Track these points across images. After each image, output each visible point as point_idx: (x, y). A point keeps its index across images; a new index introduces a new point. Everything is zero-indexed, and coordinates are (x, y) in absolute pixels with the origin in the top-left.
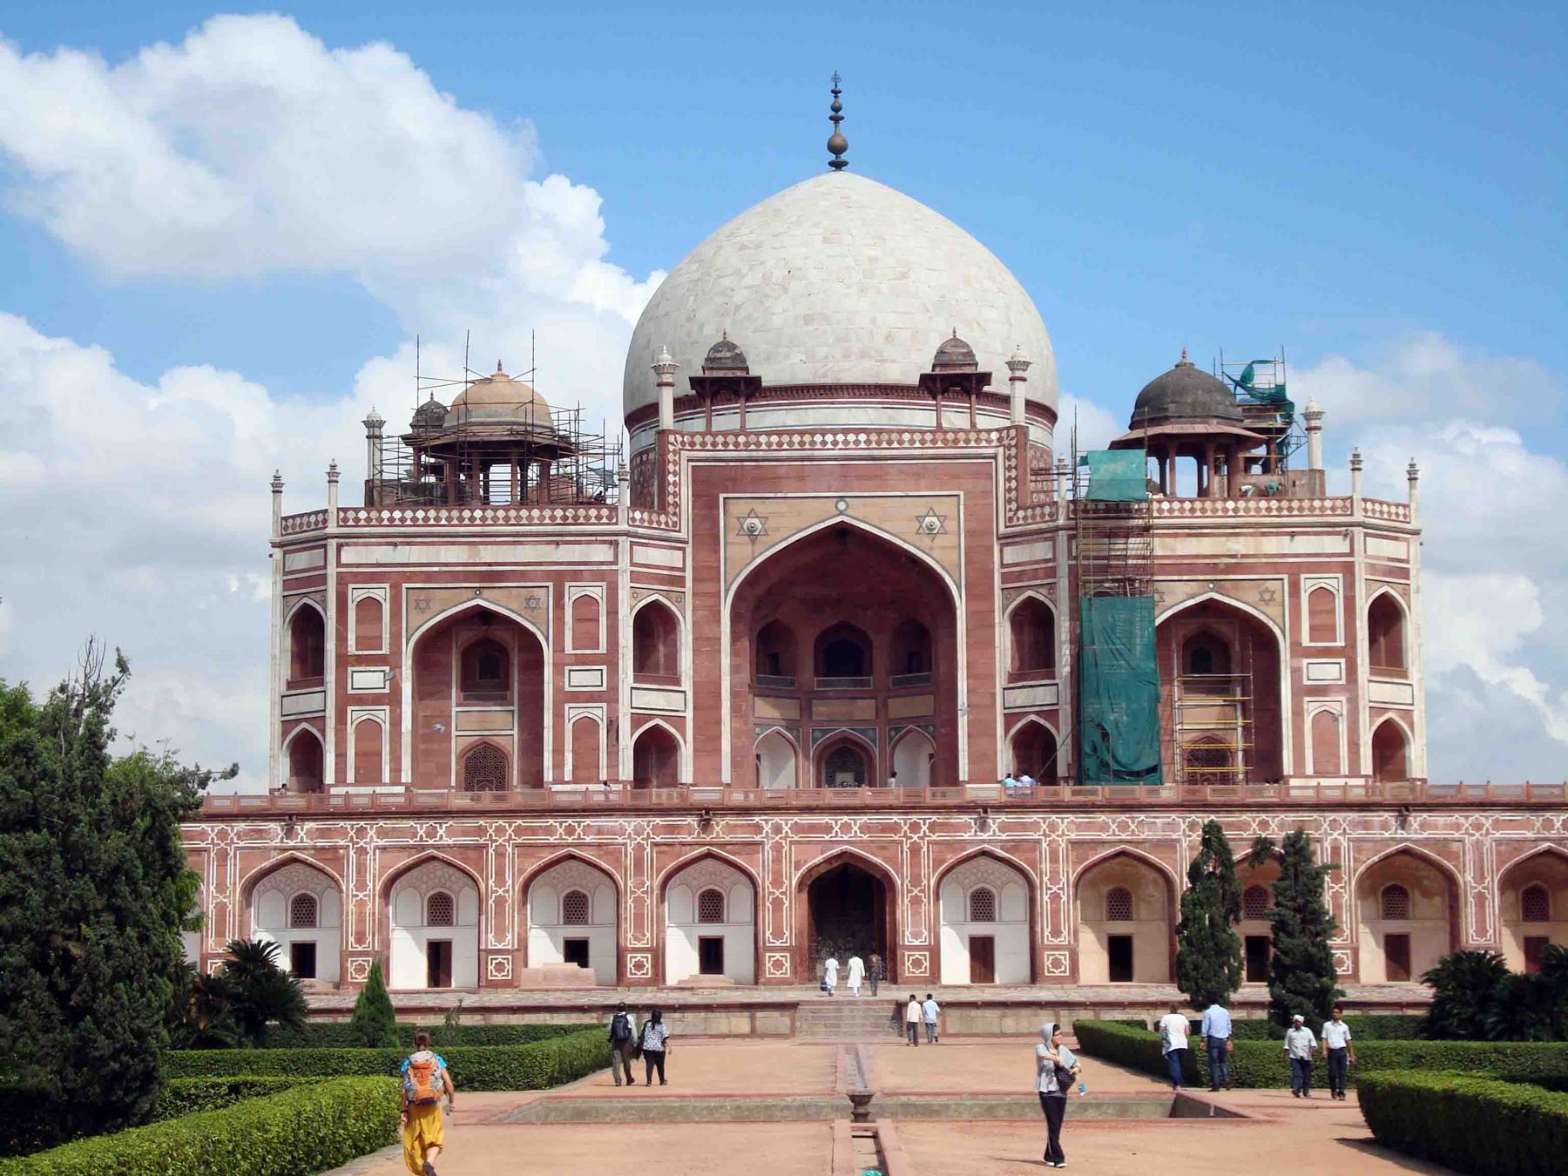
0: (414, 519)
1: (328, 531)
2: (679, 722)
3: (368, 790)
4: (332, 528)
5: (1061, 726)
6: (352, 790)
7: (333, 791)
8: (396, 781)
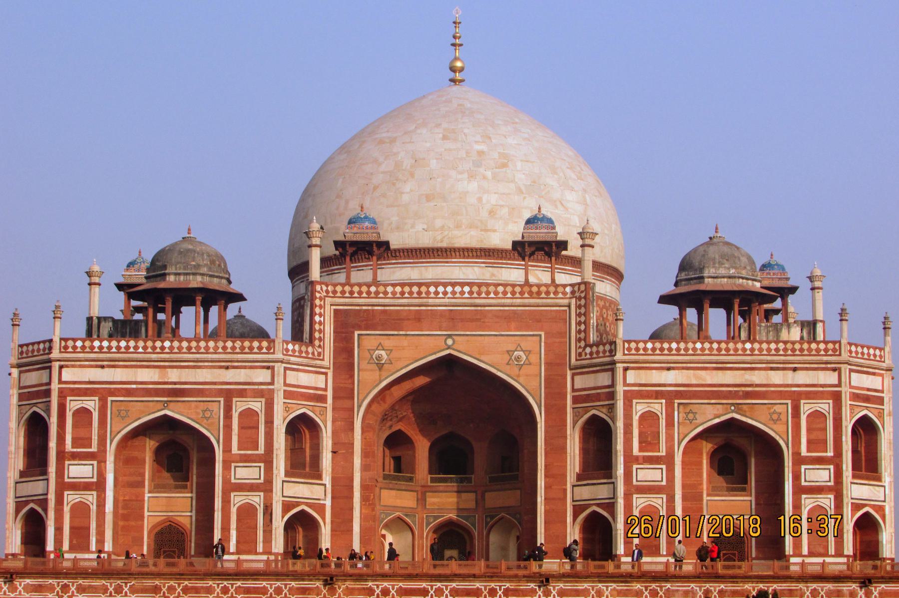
0: (242, 348)
1: (615, 358)
2: (880, 509)
3: (819, 560)
4: (619, 356)
5: (887, 518)
6: (809, 560)
7: (793, 560)
8: (839, 553)
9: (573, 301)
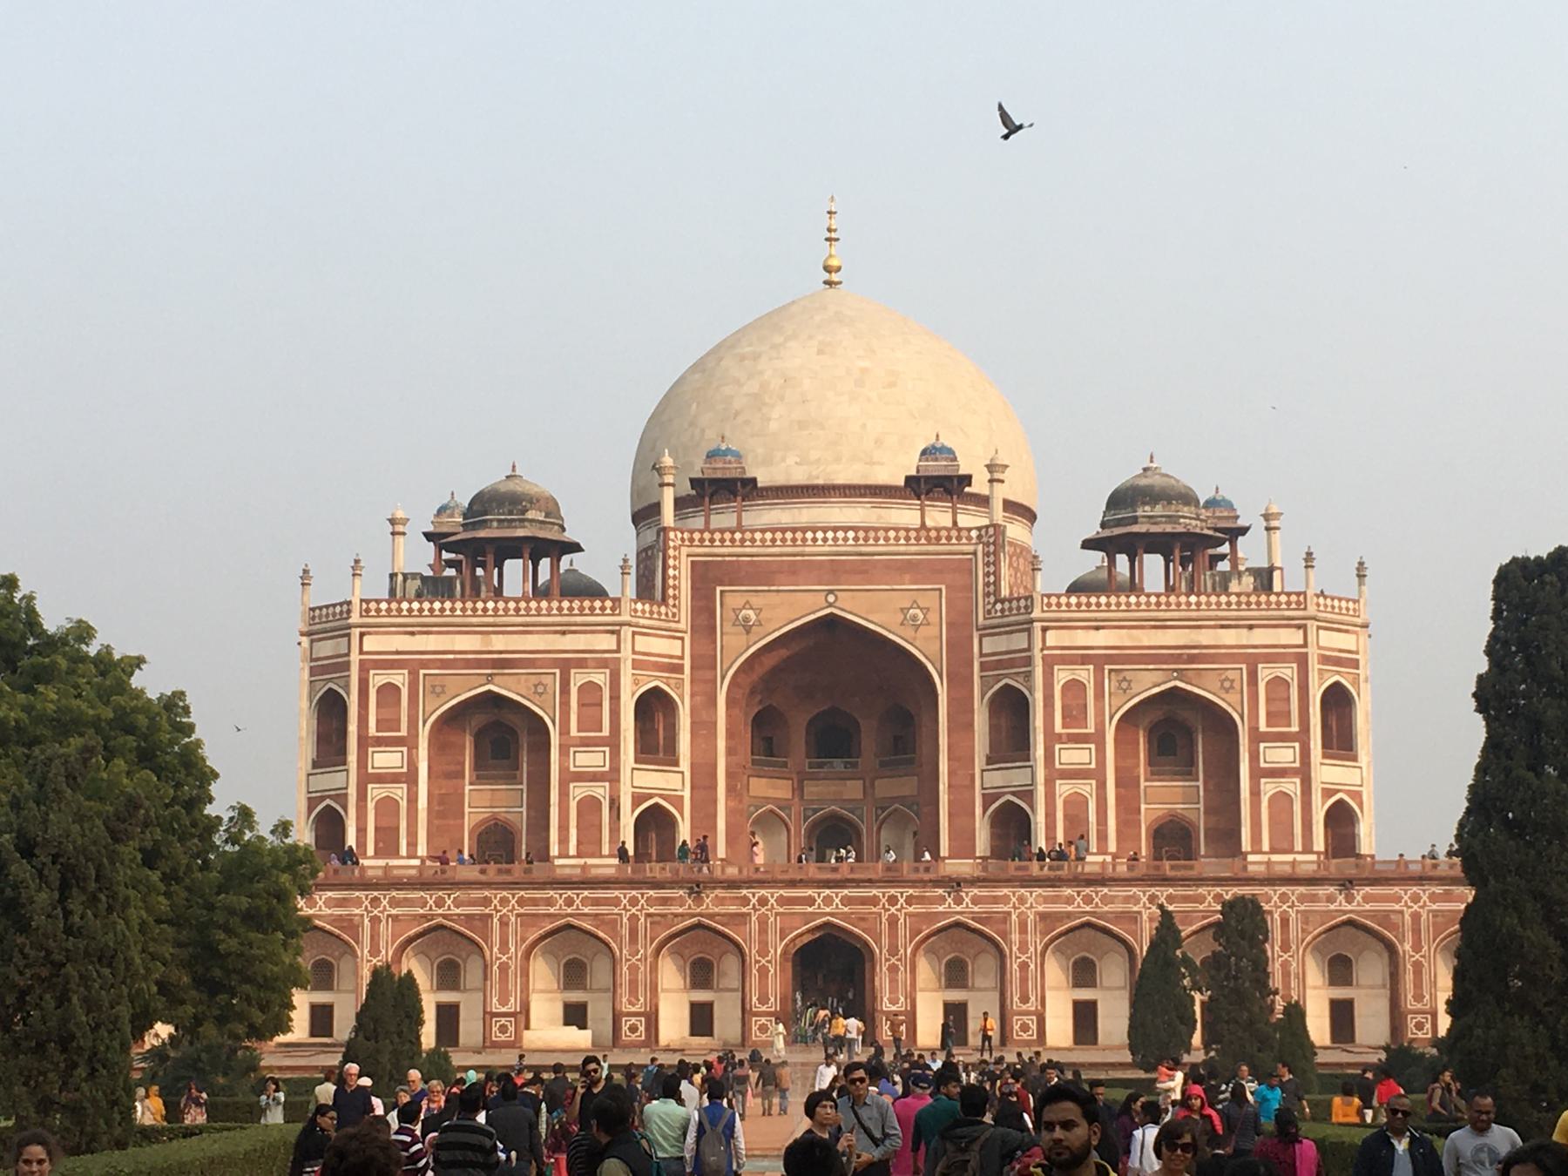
9: (685, 551)
